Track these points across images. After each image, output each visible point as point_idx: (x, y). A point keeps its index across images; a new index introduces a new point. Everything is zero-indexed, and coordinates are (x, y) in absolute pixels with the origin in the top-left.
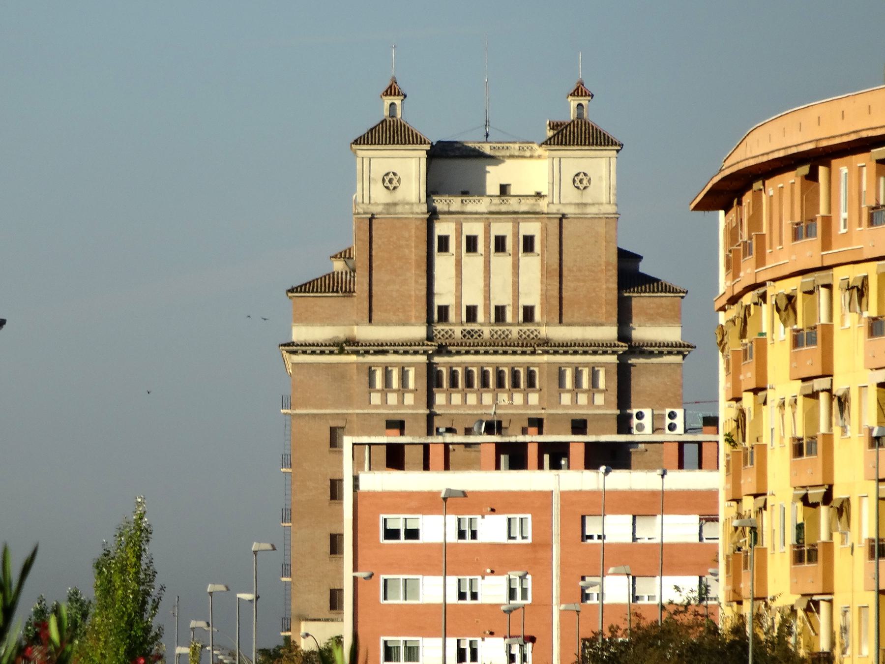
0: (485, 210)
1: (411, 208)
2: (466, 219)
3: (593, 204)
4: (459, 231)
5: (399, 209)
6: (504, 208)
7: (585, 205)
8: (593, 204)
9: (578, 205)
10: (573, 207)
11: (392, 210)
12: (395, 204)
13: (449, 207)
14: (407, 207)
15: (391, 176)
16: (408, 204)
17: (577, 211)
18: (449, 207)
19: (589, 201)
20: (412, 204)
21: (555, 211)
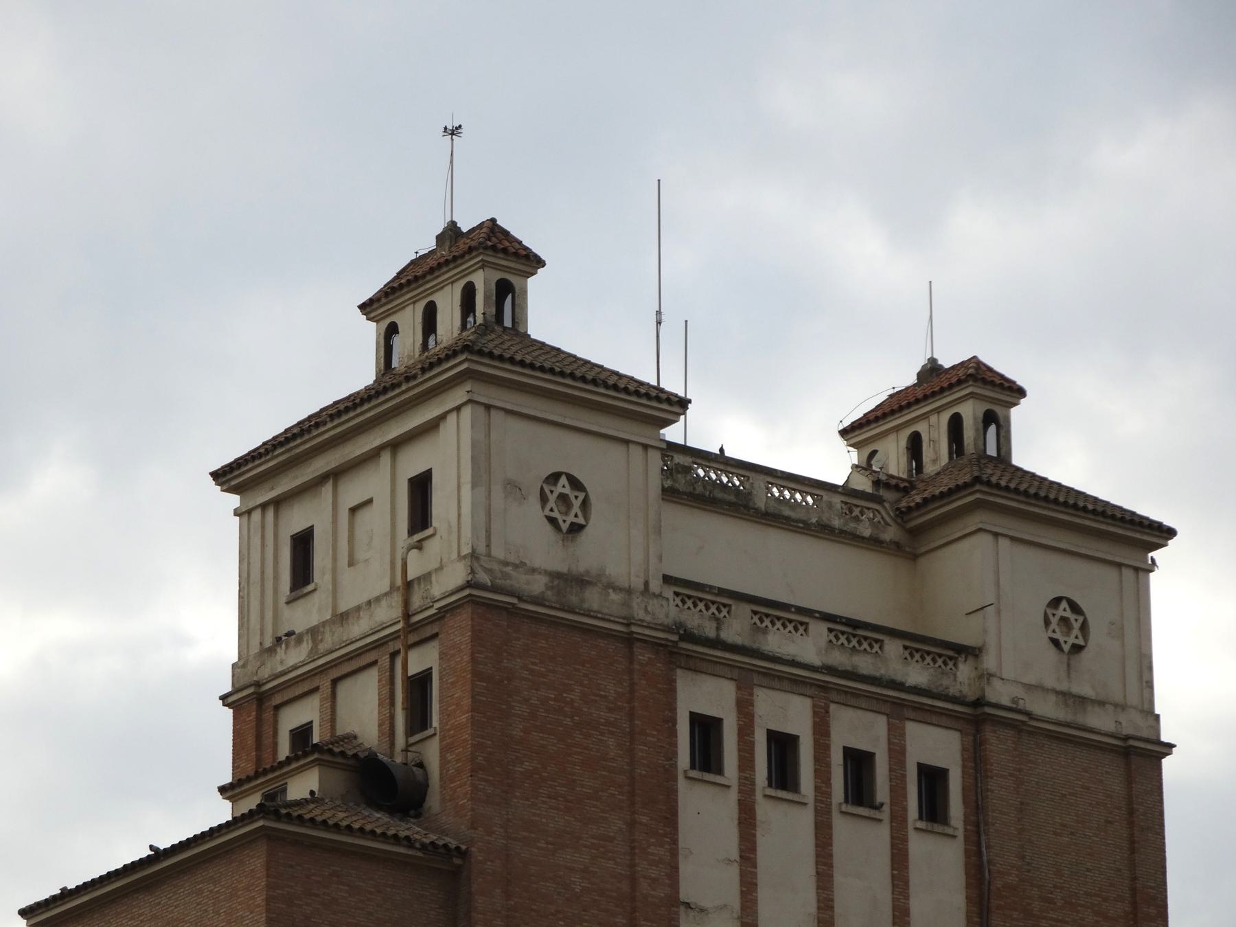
0: (817, 662)
1: (626, 604)
2: (767, 674)
3: (1102, 703)
4: (745, 708)
5: (592, 598)
6: (864, 664)
7: (1082, 701)
8: (1102, 703)
9: (1065, 696)
10: (1052, 698)
11: (574, 599)
12: (581, 581)
13: (718, 629)
14: (614, 596)
15: (563, 486)
16: (611, 586)
17: (1062, 714)
18: (718, 629)
19: (1086, 690)
20: (629, 591)
21: (1006, 701)
